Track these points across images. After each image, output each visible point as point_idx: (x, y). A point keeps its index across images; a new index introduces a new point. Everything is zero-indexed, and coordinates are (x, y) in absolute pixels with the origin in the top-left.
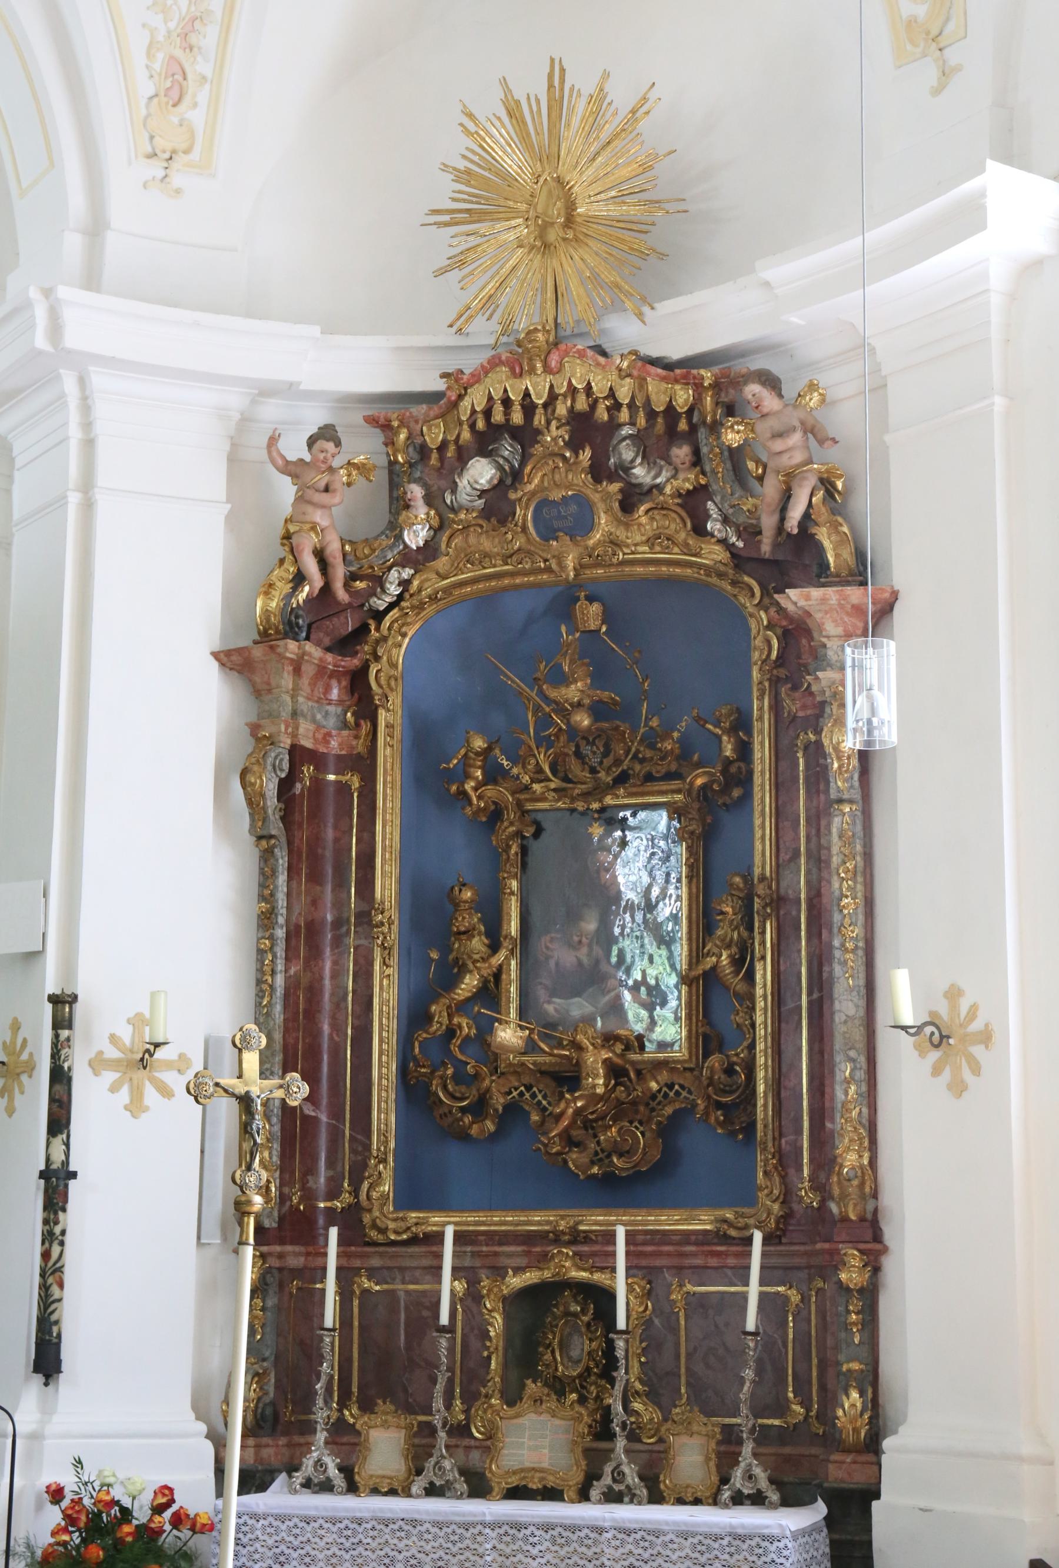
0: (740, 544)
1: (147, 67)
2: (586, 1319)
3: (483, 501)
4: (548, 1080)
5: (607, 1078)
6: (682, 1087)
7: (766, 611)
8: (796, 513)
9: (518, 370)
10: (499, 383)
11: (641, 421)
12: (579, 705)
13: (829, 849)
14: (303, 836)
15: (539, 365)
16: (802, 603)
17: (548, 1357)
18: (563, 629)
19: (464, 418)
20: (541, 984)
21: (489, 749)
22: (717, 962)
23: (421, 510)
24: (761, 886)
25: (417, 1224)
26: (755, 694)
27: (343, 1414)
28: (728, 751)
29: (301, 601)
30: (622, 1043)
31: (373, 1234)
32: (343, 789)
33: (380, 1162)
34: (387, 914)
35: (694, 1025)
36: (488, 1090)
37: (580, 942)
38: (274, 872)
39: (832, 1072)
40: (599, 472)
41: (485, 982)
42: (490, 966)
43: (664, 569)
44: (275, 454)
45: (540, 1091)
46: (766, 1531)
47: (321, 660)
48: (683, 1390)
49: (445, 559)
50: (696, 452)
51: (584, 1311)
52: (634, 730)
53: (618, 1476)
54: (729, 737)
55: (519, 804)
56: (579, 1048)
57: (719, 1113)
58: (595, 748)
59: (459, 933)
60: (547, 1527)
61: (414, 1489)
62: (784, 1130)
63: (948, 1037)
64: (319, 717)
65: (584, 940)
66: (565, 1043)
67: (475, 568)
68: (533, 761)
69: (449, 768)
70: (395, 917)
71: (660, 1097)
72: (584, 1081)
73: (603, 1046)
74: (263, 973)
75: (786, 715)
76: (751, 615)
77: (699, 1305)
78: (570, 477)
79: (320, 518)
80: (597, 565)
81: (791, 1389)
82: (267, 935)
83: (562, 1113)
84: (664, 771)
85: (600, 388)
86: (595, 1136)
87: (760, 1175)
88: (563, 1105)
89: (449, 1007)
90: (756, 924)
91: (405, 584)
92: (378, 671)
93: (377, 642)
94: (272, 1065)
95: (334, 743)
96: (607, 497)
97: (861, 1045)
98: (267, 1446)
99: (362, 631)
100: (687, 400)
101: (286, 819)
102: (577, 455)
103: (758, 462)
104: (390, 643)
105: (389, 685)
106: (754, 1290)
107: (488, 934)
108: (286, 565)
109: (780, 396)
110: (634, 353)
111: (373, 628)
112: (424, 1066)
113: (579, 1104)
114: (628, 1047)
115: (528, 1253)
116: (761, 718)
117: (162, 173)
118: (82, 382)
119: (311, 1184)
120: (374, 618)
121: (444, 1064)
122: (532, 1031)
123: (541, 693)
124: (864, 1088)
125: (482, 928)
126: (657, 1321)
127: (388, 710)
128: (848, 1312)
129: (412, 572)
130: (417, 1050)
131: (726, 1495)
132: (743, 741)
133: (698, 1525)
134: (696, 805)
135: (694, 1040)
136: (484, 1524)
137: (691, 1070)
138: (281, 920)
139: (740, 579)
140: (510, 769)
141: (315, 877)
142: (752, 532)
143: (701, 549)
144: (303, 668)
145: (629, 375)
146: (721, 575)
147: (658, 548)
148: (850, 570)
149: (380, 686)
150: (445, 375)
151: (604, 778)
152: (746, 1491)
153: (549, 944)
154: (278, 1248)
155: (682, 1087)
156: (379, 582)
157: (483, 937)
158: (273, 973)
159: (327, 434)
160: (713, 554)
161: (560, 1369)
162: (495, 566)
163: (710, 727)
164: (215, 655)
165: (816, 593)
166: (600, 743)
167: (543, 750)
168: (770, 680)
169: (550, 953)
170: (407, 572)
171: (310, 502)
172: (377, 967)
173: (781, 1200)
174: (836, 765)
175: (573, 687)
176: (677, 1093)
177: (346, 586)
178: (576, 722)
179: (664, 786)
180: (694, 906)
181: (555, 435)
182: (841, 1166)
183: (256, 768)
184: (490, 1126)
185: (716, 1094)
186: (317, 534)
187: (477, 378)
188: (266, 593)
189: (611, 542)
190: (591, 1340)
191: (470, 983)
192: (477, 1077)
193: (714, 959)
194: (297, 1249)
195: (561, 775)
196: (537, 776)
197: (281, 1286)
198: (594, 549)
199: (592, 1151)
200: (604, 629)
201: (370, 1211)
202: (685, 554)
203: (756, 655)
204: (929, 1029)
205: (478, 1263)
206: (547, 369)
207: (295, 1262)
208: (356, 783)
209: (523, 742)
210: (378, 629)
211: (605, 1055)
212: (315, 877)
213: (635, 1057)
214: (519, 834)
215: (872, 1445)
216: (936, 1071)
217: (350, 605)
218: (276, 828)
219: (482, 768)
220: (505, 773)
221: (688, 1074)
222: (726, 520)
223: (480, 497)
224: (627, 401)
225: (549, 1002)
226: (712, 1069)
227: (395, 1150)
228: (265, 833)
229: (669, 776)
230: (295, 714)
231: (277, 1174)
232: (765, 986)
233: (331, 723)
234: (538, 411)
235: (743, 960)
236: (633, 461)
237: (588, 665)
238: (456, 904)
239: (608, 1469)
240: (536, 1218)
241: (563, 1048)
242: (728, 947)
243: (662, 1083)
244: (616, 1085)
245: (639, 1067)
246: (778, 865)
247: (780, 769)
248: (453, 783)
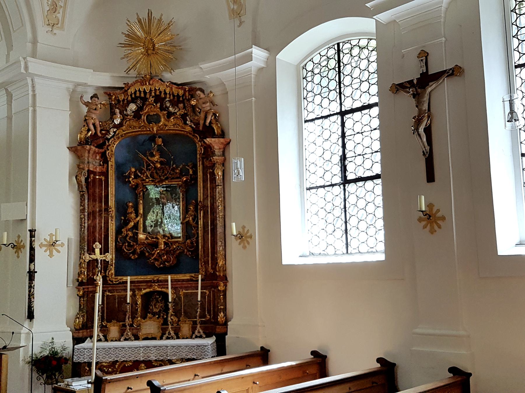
0: (195, 127)
1: (47, 3)
2: (160, 299)
3: (133, 114)
6: (181, 247)
7: (201, 142)
8: (208, 121)
9: (142, 84)
10: (137, 87)
11: (172, 98)
13: (216, 196)
14: (91, 191)
15: (147, 83)
16: (210, 141)
17: (151, 308)
18: (153, 144)
19: (129, 94)
23: (119, 115)
24: (200, 203)
25: (120, 280)
26: (198, 161)
27: (102, 324)
28: (191, 173)
29: (89, 136)
31: (109, 282)
32: (100, 180)
34: (112, 209)
36: (136, 248)
38: (84, 200)
39: (217, 244)
40: (162, 109)
42: (136, 220)
43: (177, 132)
44: (82, 100)
46: (205, 344)
47: (95, 150)
48: (183, 314)
49: (124, 127)
50: (184, 105)
51: (160, 297)
52: (170, 167)
53: (169, 334)
55: (143, 183)
56: (158, 239)
59: (129, 213)
60: (155, 347)
61: (121, 340)
63: (243, 237)
64: (94, 163)
68: (146, 174)
71: (176, 249)
74: (82, 223)
76: (197, 143)
77: (186, 295)
78: (155, 109)
79: (94, 116)
80: (162, 130)
81: (207, 312)
82: (83, 214)
83: (154, 253)
85: (162, 89)
87: (200, 266)
88: (154, 251)
90: (199, 212)
91: (115, 132)
92: (108, 153)
94: (85, 245)
95: (98, 169)
96: (164, 115)
97: (223, 238)
98: (85, 332)
99: (104, 143)
100: (182, 93)
101: (87, 187)
102: (157, 105)
103: (199, 109)
104: (111, 146)
106: (199, 291)
107: (135, 213)
108: (85, 127)
109: (204, 94)
110: (170, 81)
113: (158, 251)
116: (200, 166)
117: (51, 29)
118: (32, 80)
119: (94, 271)
121: (126, 243)
122: (147, 235)
124: (224, 247)
125: (134, 212)
126: (177, 299)
128: (220, 296)
130: (119, 240)
131: (194, 336)
133: (189, 344)
136: (140, 347)
138: (86, 211)
141: (94, 200)
142: (197, 124)
144: (90, 152)
145: (169, 87)
146: (190, 134)
147: (175, 127)
149: (109, 156)
150: (124, 84)
152: (198, 335)
154: (87, 287)
155: (181, 246)
156: (108, 132)
157: (134, 214)
158: (85, 223)
159: (95, 96)
160: (188, 129)
161: (154, 310)
162: (137, 129)
163: (186, 167)
164: (68, 148)
165: (213, 139)
167: (148, 171)
168: (201, 158)
170: (115, 130)
171: (92, 112)
174: (217, 178)
177: (100, 132)
179: (176, 180)
181: (152, 100)
182: (219, 264)
183: (80, 175)
186: (93, 120)
187: (132, 85)
188: (81, 133)
189: (165, 125)
190: (161, 304)
191: (132, 224)
192: (133, 245)
194: (91, 286)
197: (88, 295)
198: (161, 126)
200: (162, 144)
201: (109, 277)
203: (198, 152)
204: (239, 235)
205: (135, 288)
206: (149, 84)
207: (90, 290)
208: (103, 178)
209: (143, 170)
212: (94, 200)
213: (170, 240)
214: (143, 190)
215: (225, 324)
216: (240, 244)
217: (101, 137)
218: (85, 189)
220: (140, 177)
222: (191, 121)
223: (133, 113)
224: (168, 93)
226: (188, 243)
227: (115, 263)
228: (82, 190)
229: (177, 178)
230: (88, 162)
231: (86, 269)
232: (201, 225)
233: (97, 164)
235: (196, 218)
236: (169, 106)
237: (159, 153)
238: (128, 206)
239: (167, 332)
242: (192, 216)
246: (204, 199)
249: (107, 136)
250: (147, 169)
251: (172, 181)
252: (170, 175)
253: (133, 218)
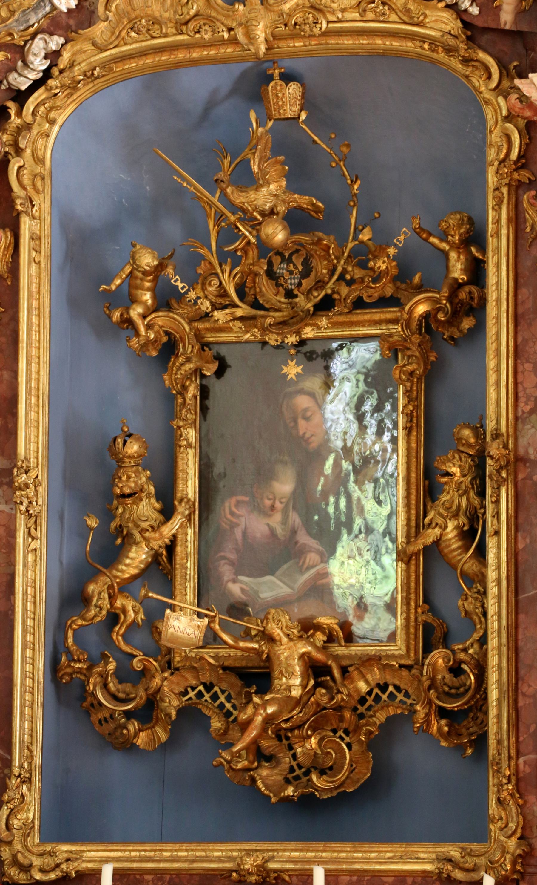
0: (475, 10)
5: (305, 677)
6: (398, 688)
7: (506, 98)
12: (272, 212)
18: (253, 116)
20: (224, 558)
21: (161, 267)
22: (441, 535)
24: (495, 445)
25: (68, 860)
26: (491, 203)
30: (324, 633)
33: (23, 782)
34: (33, 474)
35: (413, 611)
36: (159, 690)
37: (273, 508)
41: (156, 556)
42: (162, 536)
43: (379, 41)
45: (223, 692)
49: (102, 26)
52: (342, 243)
54: (459, 253)
55: (198, 336)
56: (271, 640)
57: (443, 722)
58: (291, 267)
59: (124, 496)
62: (522, 748)
65: (278, 505)
66: (253, 633)
67: (141, 37)
68: (215, 282)
69: (110, 291)
70: (43, 478)
71: (370, 701)
72: (276, 682)
73: (301, 637)
75: (528, 230)
80: (294, 36)
83: (249, 722)
84: (376, 295)
86: (290, 747)
87: (493, 802)
88: (250, 710)
89: (111, 587)
90: (489, 491)
92: (20, 168)
93: (19, 130)
104: (35, 131)
105: (34, 185)
107: (159, 497)
111: (12, 112)
112: (79, 661)
113: (270, 710)
114: (331, 638)
116: (497, 233)
120: (13, 99)
121: (104, 657)
122: (212, 619)
123: (225, 198)
125: (152, 489)
127: (34, 218)
129: (62, 40)
130: (70, 641)
132: (476, 259)
134: (416, 339)
135: (412, 631)
137: (409, 668)
139: (474, 56)
140: (186, 293)
143: (426, 16)
146: (449, 50)
147: (370, 15)
151: (303, 303)
153: (234, 509)
157: (153, 500)
162: (166, 36)
163: (434, 240)
166: (298, 261)
167: (227, 269)
168: (509, 185)
169: (234, 520)
173: (518, 835)
175: (264, 190)
176: (392, 696)
178: (267, 236)
179: (377, 315)
180: (413, 464)
184: (163, 735)
185: (438, 698)
189: (312, 7)
193: (437, 531)
195: (250, 298)
196: (219, 300)
198: (290, 15)
199: (287, 767)
200: (303, 116)
201: (9, 843)
202: (405, 23)
203: (491, 154)
209: (202, 258)
210: (19, 114)
211: (304, 648)
213: (340, 650)
214: (198, 372)
219: (153, 290)
220: (180, 297)
221: (405, 673)
225: (234, 581)
226: (434, 665)
227: (42, 767)
232: (499, 568)
237: (283, 164)
240: (216, 854)
241: (252, 639)
242: (456, 516)
243: (373, 683)
244: (317, 685)
245: (344, 663)
246: (516, 418)
247: (520, 297)
248: (116, 308)
249: (13, 77)
250: (222, 260)
251: (354, 318)
252: (344, 290)
253: (145, 525)
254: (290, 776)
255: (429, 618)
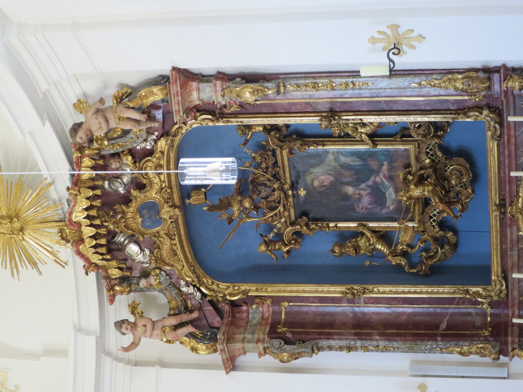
4: (427, 210)
6: (427, 148)
20: (380, 212)
22: (365, 134)
25: (498, 276)
31: (502, 295)
35: (397, 143)
37: (359, 194)
45: (432, 212)
62: (447, 108)
64: (254, 322)
65: (358, 192)
70: (349, 287)
71: (433, 158)
72: (426, 196)
75: (239, 109)
76: (191, 127)
84: (272, 157)
87: (468, 120)
112: (422, 268)
114: (410, 173)
115: (511, 226)
130: (415, 271)
137: (419, 144)
138: (353, 342)
139: (173, 133)
140: (275, 232)
146: (172, 141)
148: (164, 88)
150: (87, 274)
153: (360, 208)
155: (427, 148)
157: (358, 239)
160: (162, 144)
163: (249, 137)
169: (364, 208)
172: (374, 296)
173: (481, 110)
176: (431, 150)
185: (430, 134)
187: (87, 260)
193: (363, 136)
195: (277, 204)
196: (278, 216)
199: (461, 188)
205: (516, 248)
208: (286, 304)
216: (413, 47)
221: (421, 146)
225: (389, 208)
234: (100, 232)
240: (494, 222)
242: (357, 129)
243: (426, 157)
245: (418, 168)
247: (266, 112)
253: (368, 244)
254: (464, 188)
255: (398, 136)
